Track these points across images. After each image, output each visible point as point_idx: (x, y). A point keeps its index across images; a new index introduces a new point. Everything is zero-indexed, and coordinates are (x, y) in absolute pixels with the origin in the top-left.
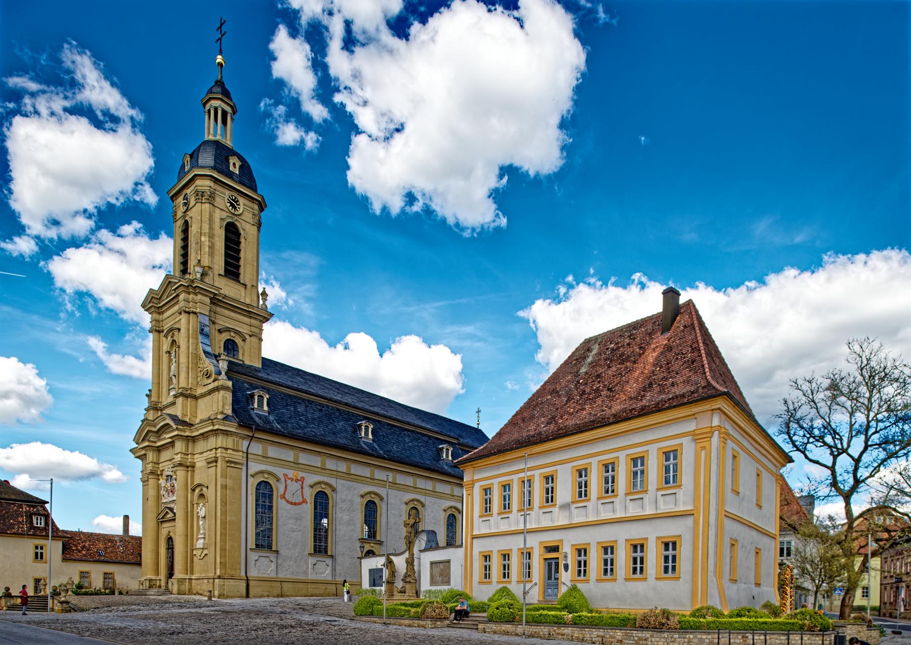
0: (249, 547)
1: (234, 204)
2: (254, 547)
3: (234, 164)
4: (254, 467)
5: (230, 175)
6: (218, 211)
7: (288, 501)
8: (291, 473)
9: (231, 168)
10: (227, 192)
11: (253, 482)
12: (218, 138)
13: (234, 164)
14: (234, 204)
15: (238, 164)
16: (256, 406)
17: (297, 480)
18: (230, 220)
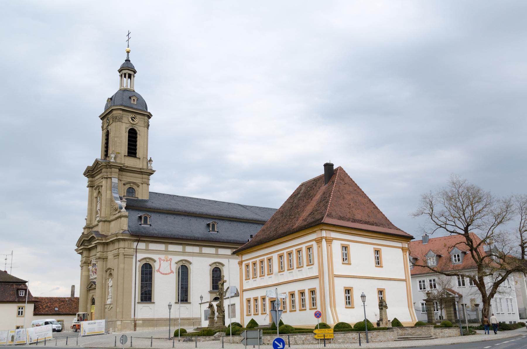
0: (137, 301)
2: (140, 301)
4: (140, 256)
7: (161, 273)
8: (163, 257)
11: (139, 265)
17: (167, 261)
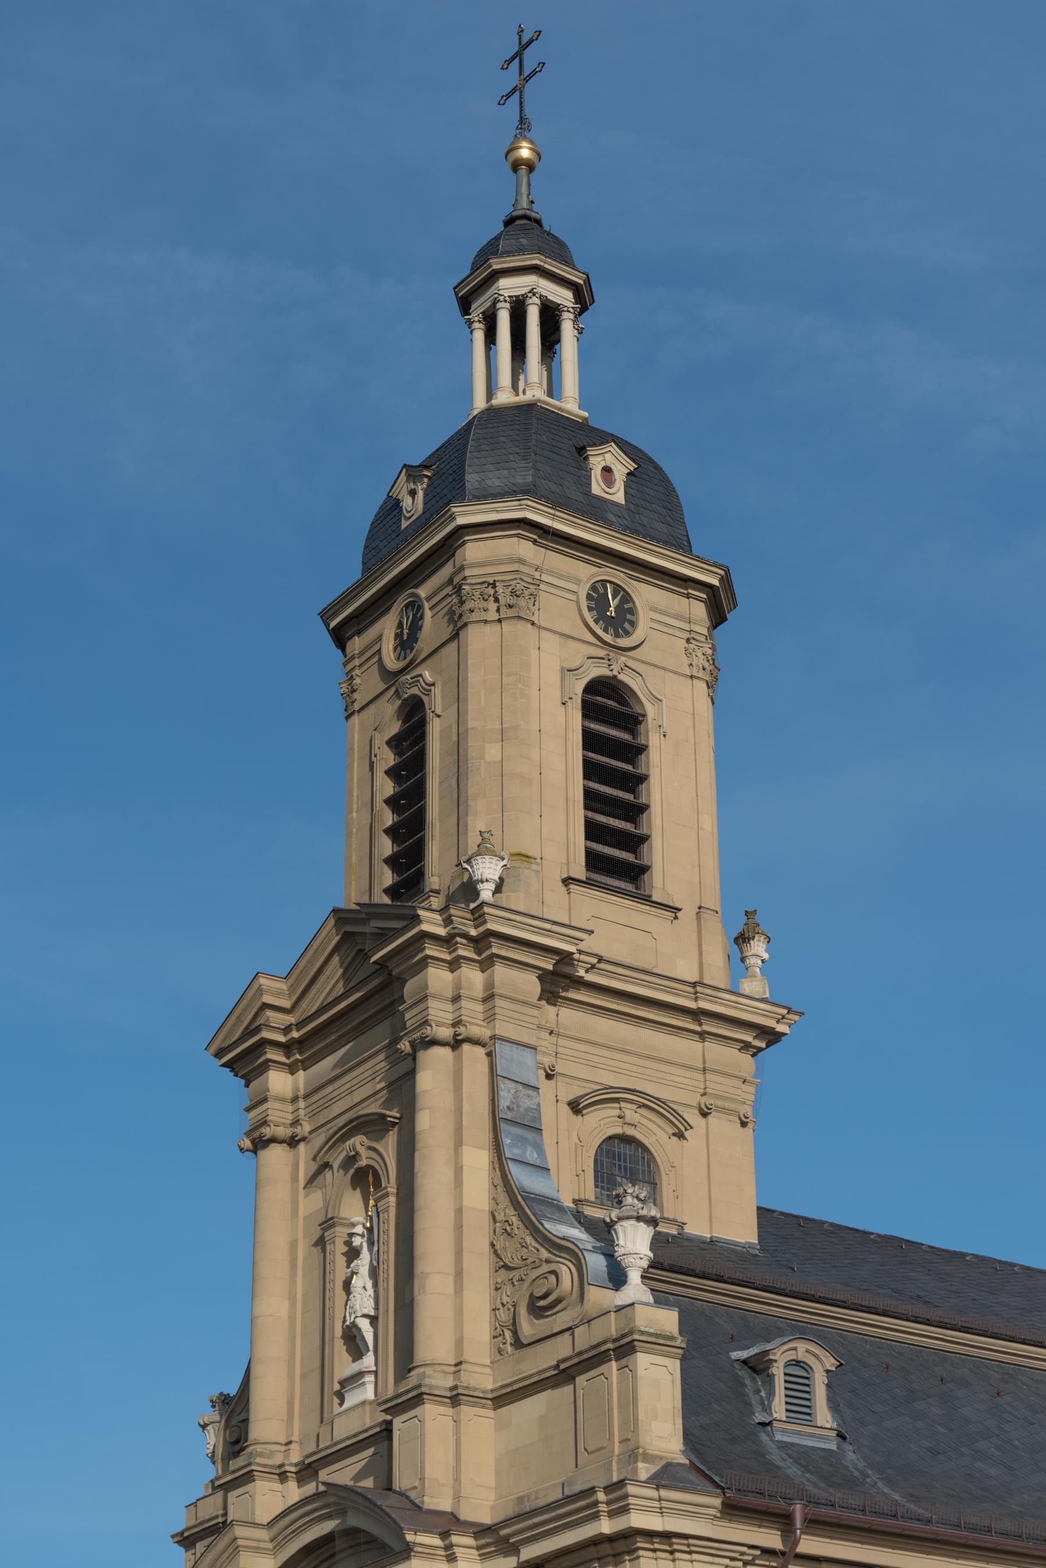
1: (613, 616)
3: (607, 470)
5: (595, 510)
6: (550, 642)
9: (597, 488)
10: (585, 573)
12: (534, 390)
13: (607, 470)
14: (613, 616)
15: (622, 466)
16: (779, 1409)
18: (604, 671)
